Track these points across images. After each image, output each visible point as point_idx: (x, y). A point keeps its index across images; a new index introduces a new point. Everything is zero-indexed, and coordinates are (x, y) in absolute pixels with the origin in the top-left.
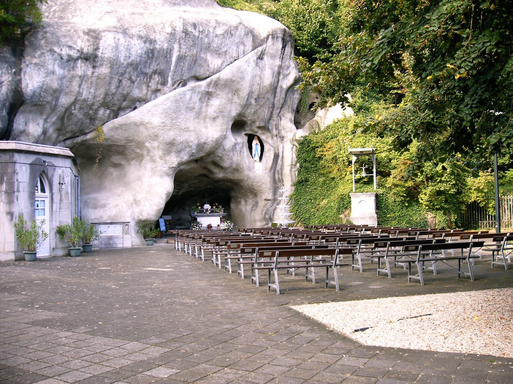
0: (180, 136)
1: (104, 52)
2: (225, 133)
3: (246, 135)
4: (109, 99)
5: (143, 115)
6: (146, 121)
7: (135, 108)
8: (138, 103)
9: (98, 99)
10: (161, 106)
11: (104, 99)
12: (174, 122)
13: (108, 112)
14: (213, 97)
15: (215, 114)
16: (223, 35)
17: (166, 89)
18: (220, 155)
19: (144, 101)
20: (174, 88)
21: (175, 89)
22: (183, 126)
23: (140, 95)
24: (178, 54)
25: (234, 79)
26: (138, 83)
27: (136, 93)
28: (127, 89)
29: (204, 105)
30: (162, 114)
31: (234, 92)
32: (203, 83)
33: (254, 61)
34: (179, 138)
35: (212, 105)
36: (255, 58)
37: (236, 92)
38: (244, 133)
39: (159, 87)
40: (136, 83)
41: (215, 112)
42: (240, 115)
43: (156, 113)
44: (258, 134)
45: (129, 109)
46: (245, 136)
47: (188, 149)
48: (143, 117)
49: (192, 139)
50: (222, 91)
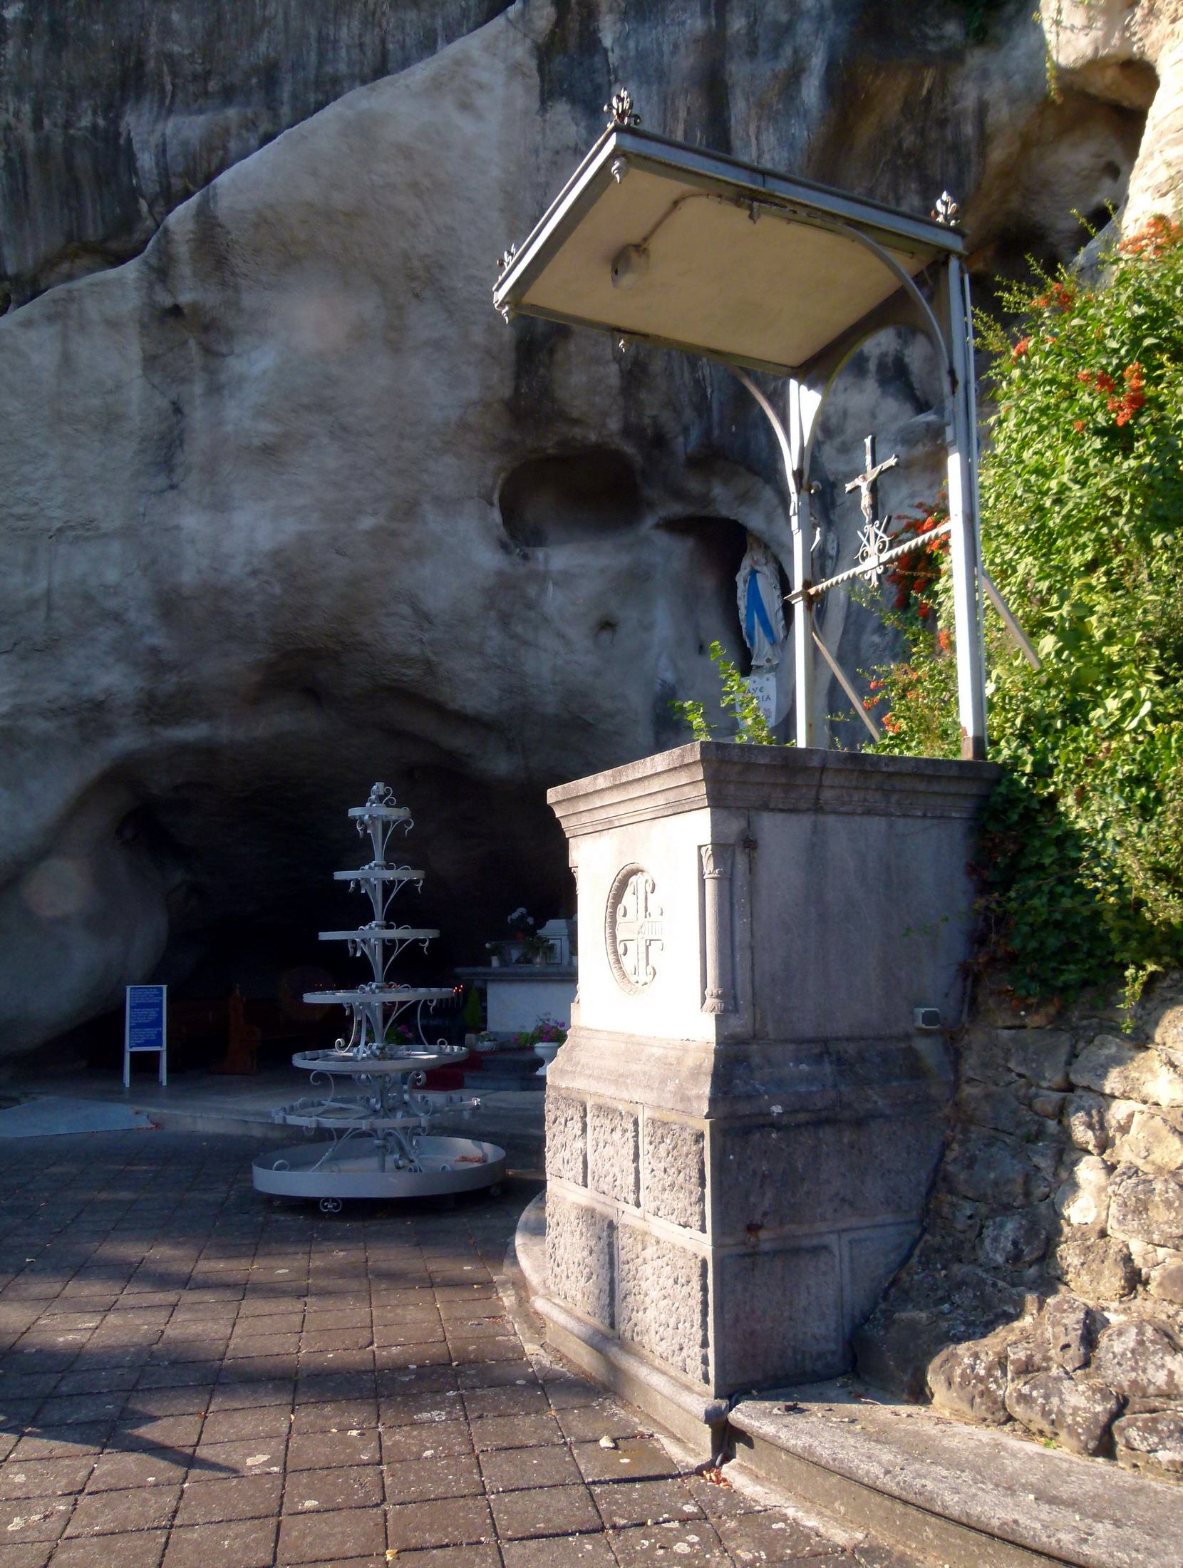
0: (29, 568)
3: (674, 526)
14: (229, 335)
15: (266, 427)
18: (414, 650)
22: (57, 515)
29: (198, 389)
32: (131, 270)
33: (515, 70)
34: (17, 579)
35: (241, 380)
36: (521, 52)
38: (649, 521)
41: (261, 412)
46: (663, 540)
47: (107, 635)
49: (112, 576)
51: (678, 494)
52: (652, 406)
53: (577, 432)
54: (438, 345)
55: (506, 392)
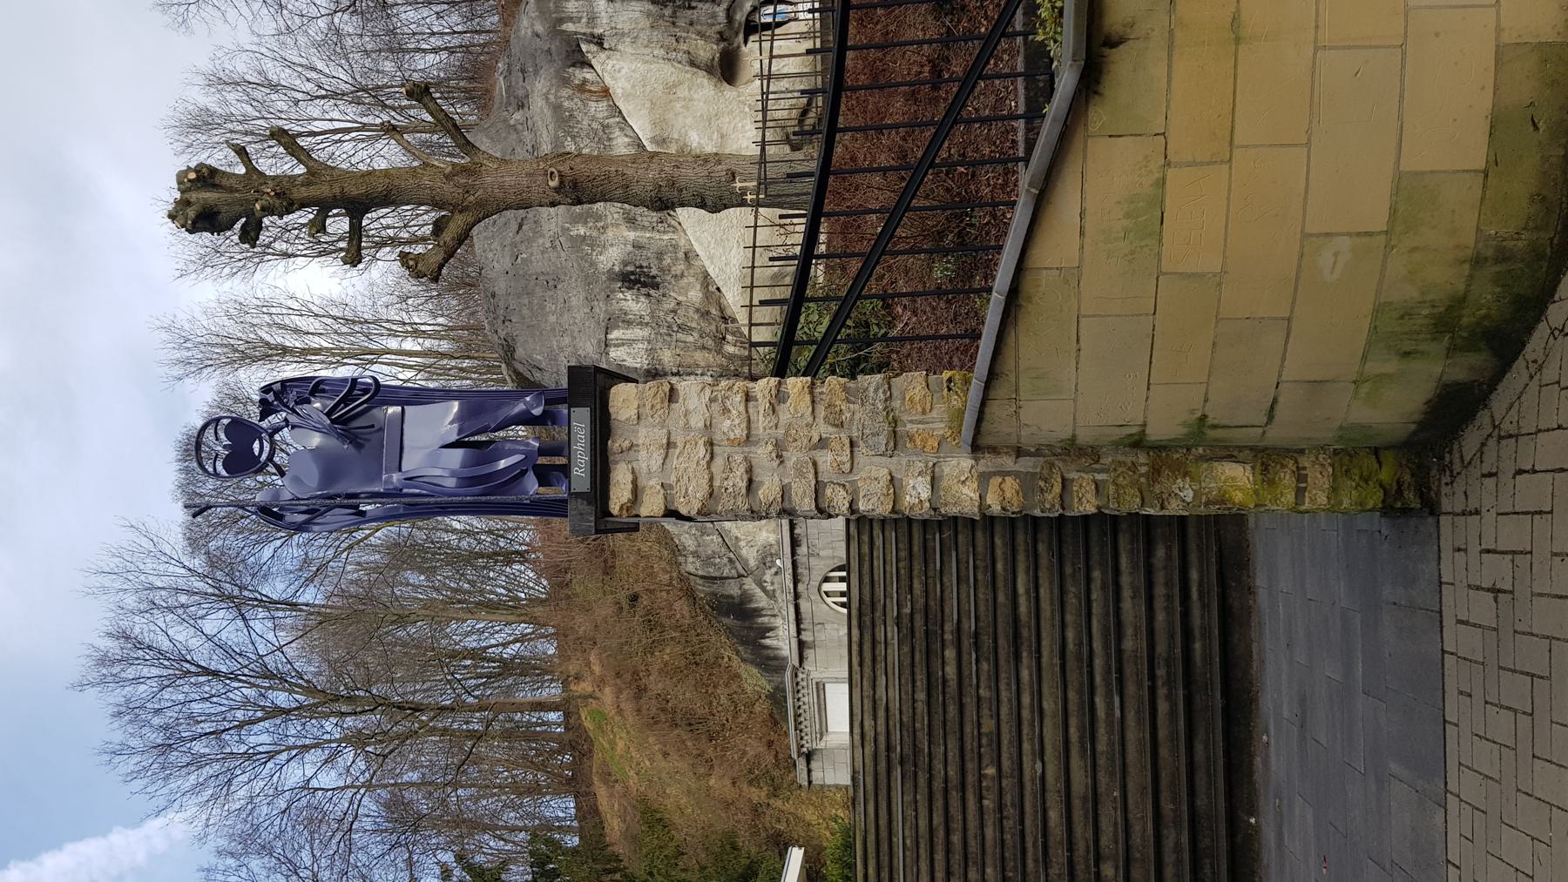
1: (639, 360)
2: (747, 109)
3: (746, 42)
4: (710, 342)
7: (718, 289)
8: (710, 287)
9: (712, 360)
10: (712, 251)
11: (710, 350)
12: (735, 221)
13: (729, 337)
16: (573, 138)
17: (682, 242)
19: (706, 278)
20: (679, 227)
21: (680, 224)
23: (698, 287)
24: (623, 227)
25: (648, 105)
26: (680, 294)
27: (695, 295)
28: (691, 312)
30: (724, 248)
31: (672, 97)
37: (671, 88)
38: (743, 48)
39: (681, 255)
40: (680, 298)
42: (709, 70)
43: (724, 258)
44: (744, 19)
45: (722, 300)
48: (732, 280)
50: (673, 126)
51: (737, 34)
52: (712, 32)
53: (716, 59)
54: (690, 89)
55: (705, 73)
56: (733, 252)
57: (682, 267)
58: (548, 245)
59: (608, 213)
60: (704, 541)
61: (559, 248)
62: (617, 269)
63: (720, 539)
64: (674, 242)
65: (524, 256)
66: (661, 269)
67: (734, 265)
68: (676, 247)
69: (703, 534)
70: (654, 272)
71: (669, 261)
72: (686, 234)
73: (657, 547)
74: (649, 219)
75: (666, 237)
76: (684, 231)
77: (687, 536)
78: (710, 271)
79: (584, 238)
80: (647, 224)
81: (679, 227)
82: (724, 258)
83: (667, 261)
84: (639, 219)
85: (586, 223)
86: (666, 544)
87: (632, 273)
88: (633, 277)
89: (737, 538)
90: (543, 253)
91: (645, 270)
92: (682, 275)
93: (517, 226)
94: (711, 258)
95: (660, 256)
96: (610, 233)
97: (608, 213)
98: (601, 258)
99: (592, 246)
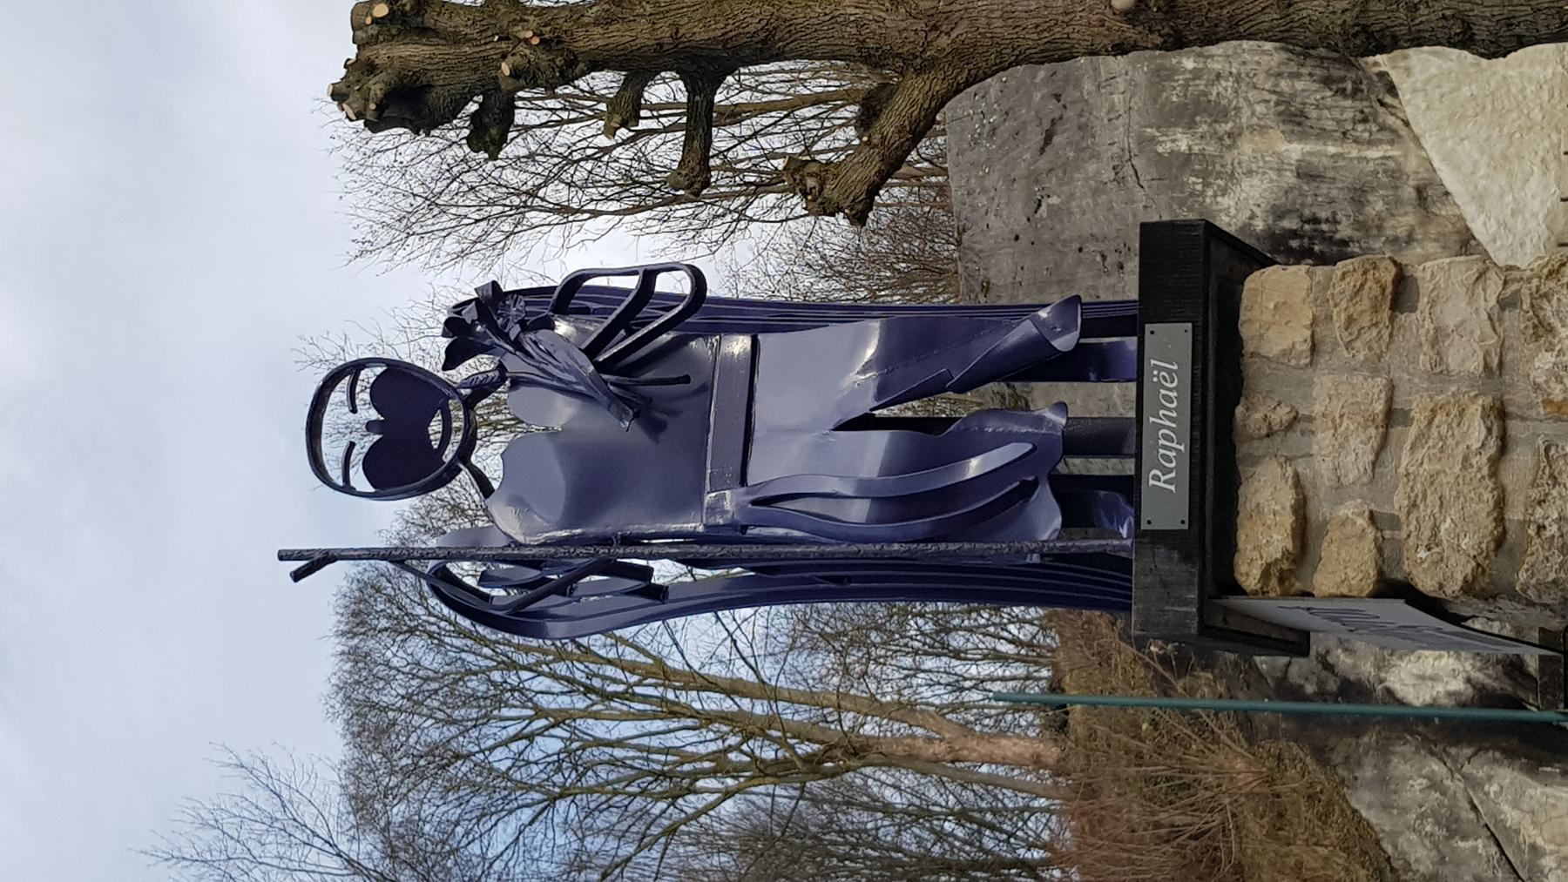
5: (1522, 245)
6: (1547, 233)
17: (1412, 164)
21: (1406, 123)
43: (1509, 198)
56: (1533, 184)
57: (1410, 219)
58: (1108, 175)
59: (1243, 104)
60: (1454, 850)
61: (1131, 180)
62: (1259, 225)
63: (1494, 850)
64: (1392, 164)
65: (1054, 200)
66: (1361, 226)
67: (1535, 215)
68: (1396, 175)
69: (1452, 834)
70: (1344, 231)
71: (1380, 206)
72: (1420, 146)
73: (1340, 859)
74: (1336, 114)
75: (1374, 153)
76: (1416, 140)
77: (1414, 837)
78: (1477, 228)
79: (1186, 159)
80: (1330, 125)
81: (1403, 131)
82: (1509, 198)
83: (1376, 206)
84: (1314, 114)
85: (1192, 125)
86: (1364, 853)
87: (1294, 234)
88: (1294, 244)
89: (1534, 848)
90: (1095, 193)
91: (1324, 227)
92: (1410, 239)
93: (1040, 138)
94: (1479, 198)
95: (1359, 195)
96: (1246, 147)
97: (1243, 104)
98: (1225, 201)
99: (1205, 175)
